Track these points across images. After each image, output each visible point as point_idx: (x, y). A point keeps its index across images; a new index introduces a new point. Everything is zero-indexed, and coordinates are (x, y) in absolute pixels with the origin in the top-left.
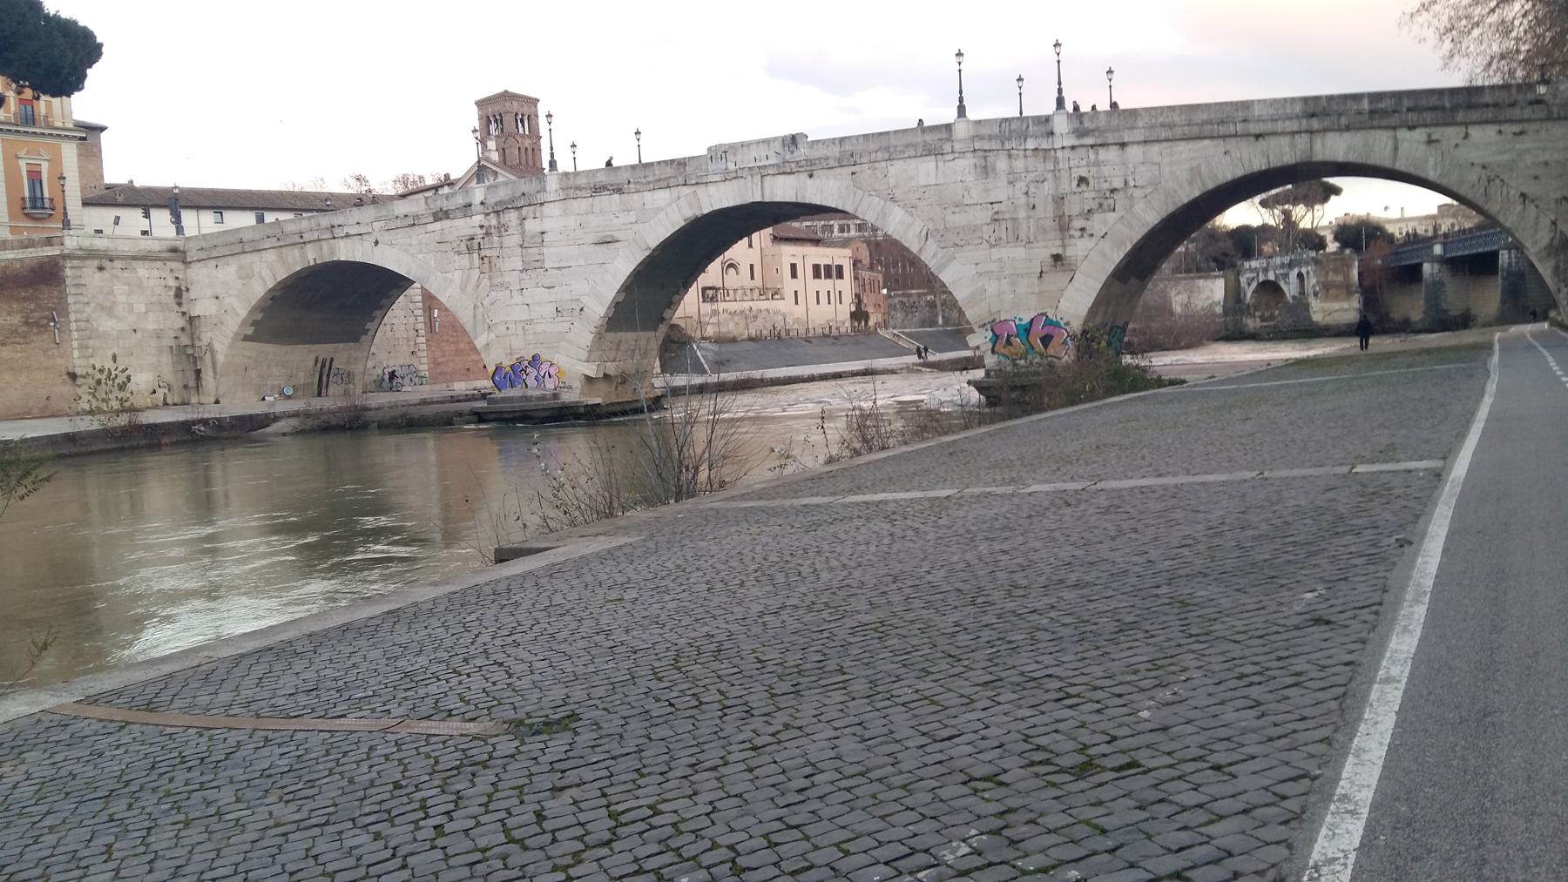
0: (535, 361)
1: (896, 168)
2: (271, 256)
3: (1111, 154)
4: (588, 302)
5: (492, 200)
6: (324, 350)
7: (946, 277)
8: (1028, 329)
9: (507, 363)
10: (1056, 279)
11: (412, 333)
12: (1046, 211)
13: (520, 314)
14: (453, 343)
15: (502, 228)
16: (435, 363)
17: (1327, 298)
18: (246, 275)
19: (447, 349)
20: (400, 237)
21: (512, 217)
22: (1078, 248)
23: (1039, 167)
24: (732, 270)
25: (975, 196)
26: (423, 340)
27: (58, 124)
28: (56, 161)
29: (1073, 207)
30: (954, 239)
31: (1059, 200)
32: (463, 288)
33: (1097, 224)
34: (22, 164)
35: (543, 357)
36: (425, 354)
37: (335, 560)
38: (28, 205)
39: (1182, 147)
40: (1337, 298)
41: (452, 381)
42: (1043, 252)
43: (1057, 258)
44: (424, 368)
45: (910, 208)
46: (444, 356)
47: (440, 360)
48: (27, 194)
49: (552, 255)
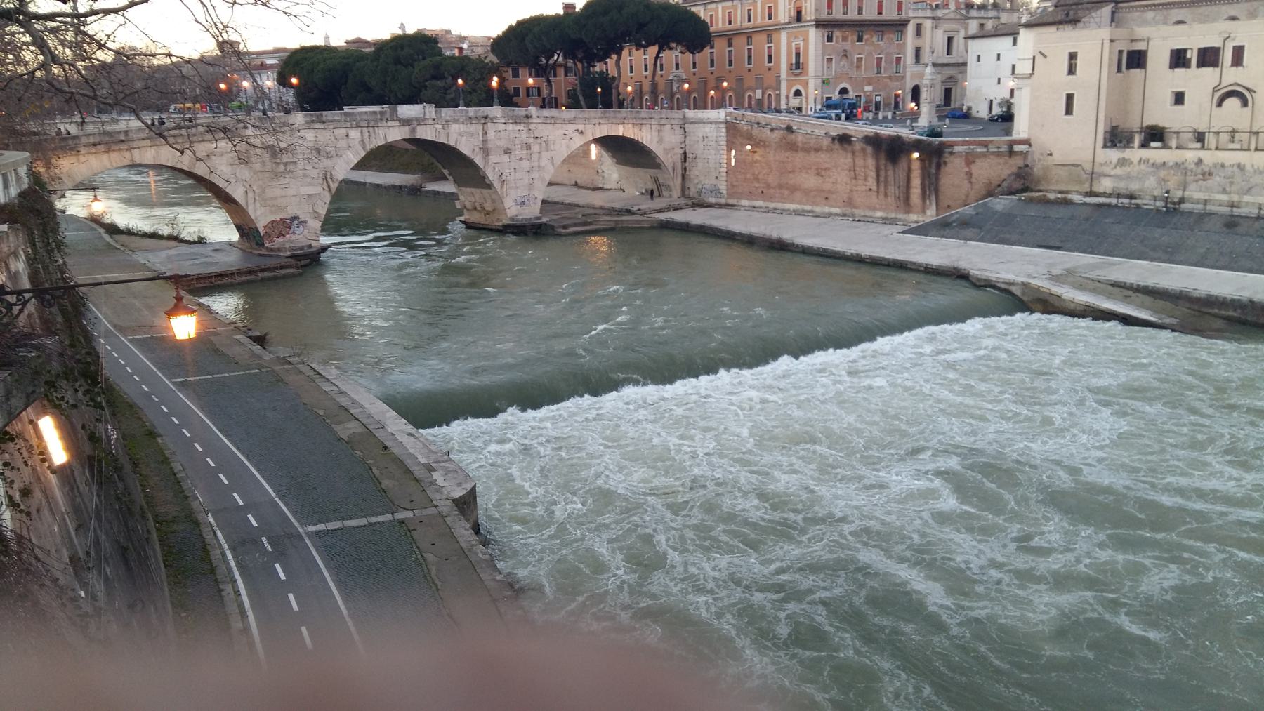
6: (652, 172)
11: (718, 165)
14: (743, 173)
16: (731, 186)
19: (739, 177)
24: (1232, 103)
26: (725, 170)
27: (808, 19)
28: (806, 40)
34: (793, 44)
36: (724, 179)
37: (520, 267)
38: (794, 67)
41: (740, 198)
44: (723, 187)
46: (737, 181)
47: (735, 184)
48: (794, 61)
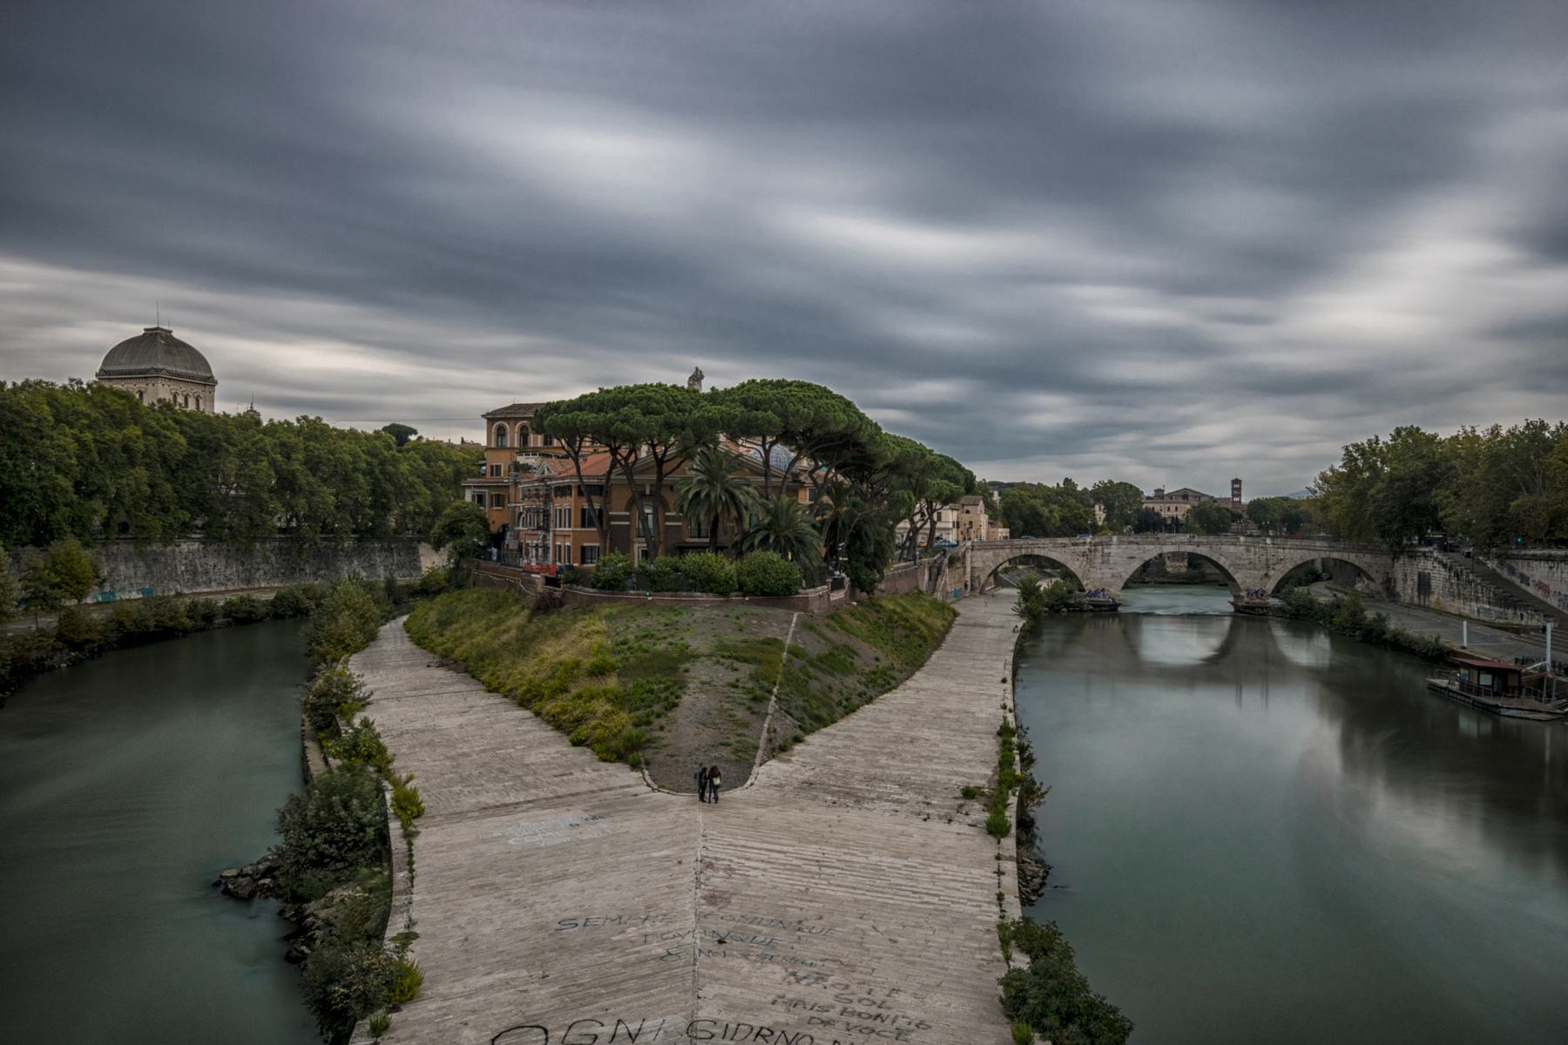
0: (1103, 590)
1: (1223, 547)
2: (1008, 551)
3: (1281, 550)
4: (1123, 574)
5: (1093, 542)
7: (1235, 577)
8: (1257, 592)
9: (1093, 590)
10: (1265, 580)
12: (1264, 562)
13: (1100, 576)
15: (1096, 550)
17: (1173, 561)
18: (996, 556)
20: (1059, 550)
21: (1100, 548)
22: (1271, 573)
23: (1262, 551)
25: (1245, 556)
29: (1271, 562)
30: (1238, 567)
31: (1267, 560)
32: (1080, 567)
33: (1277, 567)
35: (1106, 588)
39: (1299, 551)
40: (1178, 561)
42: (1263, 572)
43: (1266, 575)
45: (1227, 558)
49: (1112, 560)
